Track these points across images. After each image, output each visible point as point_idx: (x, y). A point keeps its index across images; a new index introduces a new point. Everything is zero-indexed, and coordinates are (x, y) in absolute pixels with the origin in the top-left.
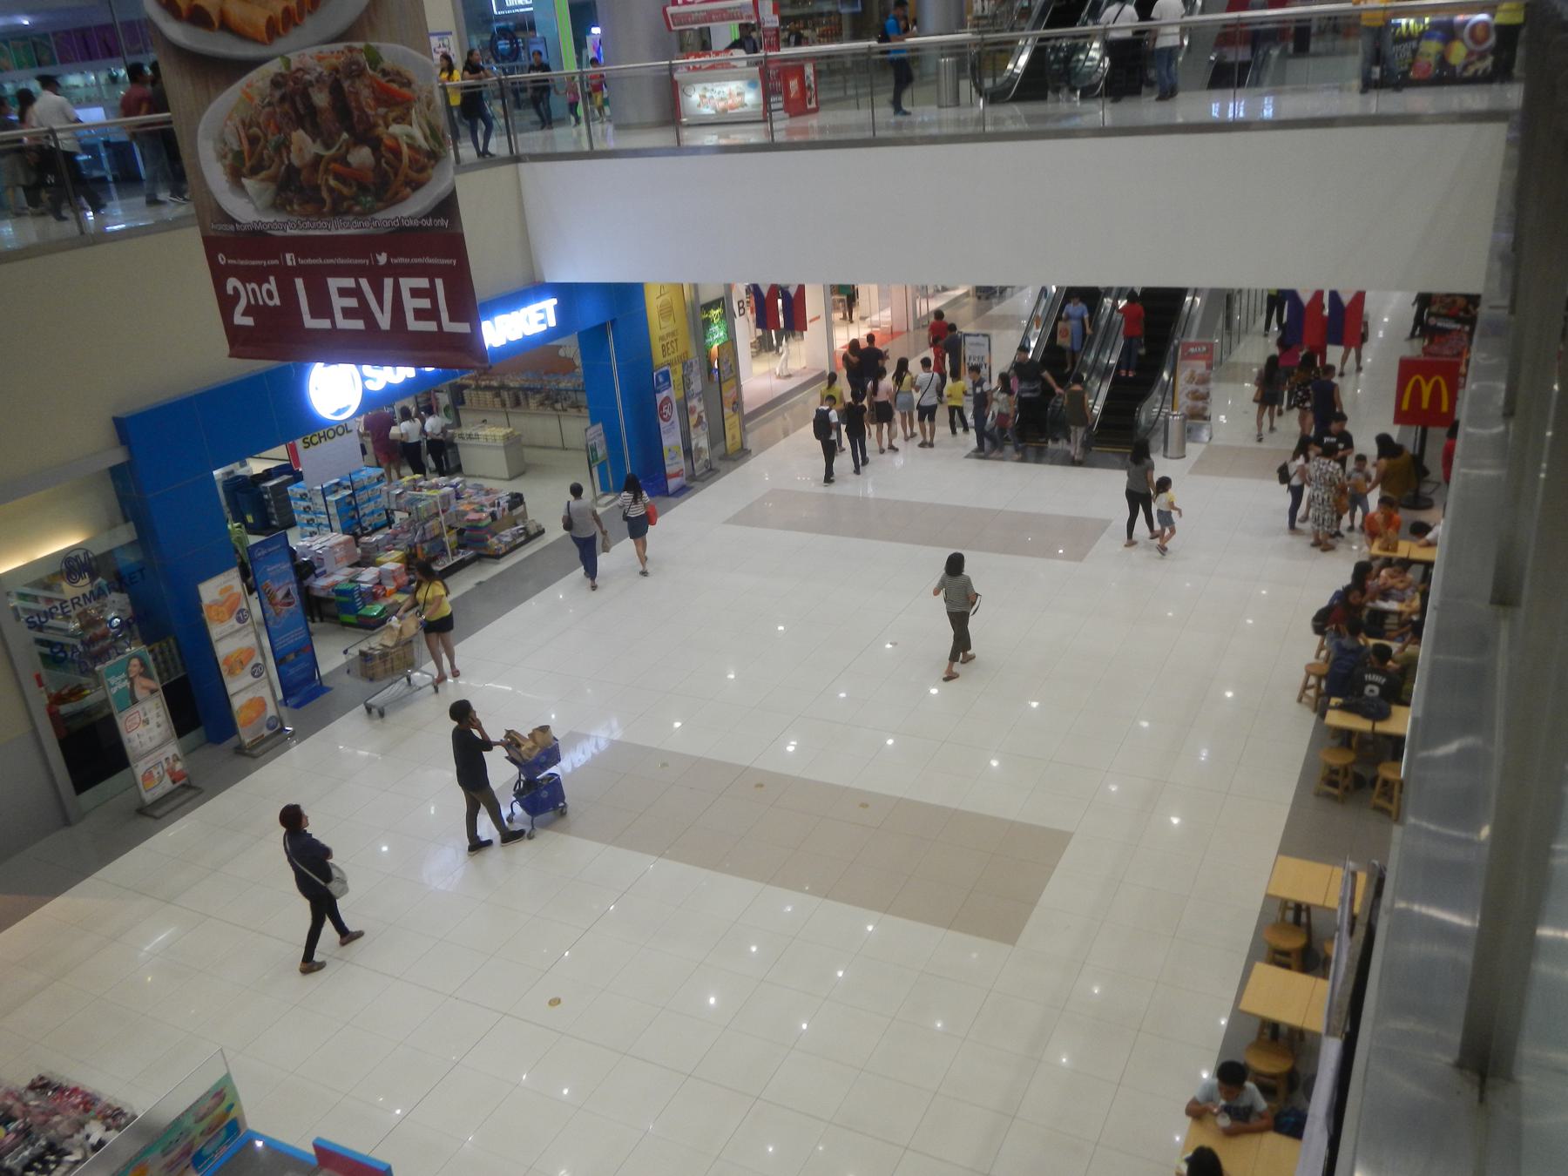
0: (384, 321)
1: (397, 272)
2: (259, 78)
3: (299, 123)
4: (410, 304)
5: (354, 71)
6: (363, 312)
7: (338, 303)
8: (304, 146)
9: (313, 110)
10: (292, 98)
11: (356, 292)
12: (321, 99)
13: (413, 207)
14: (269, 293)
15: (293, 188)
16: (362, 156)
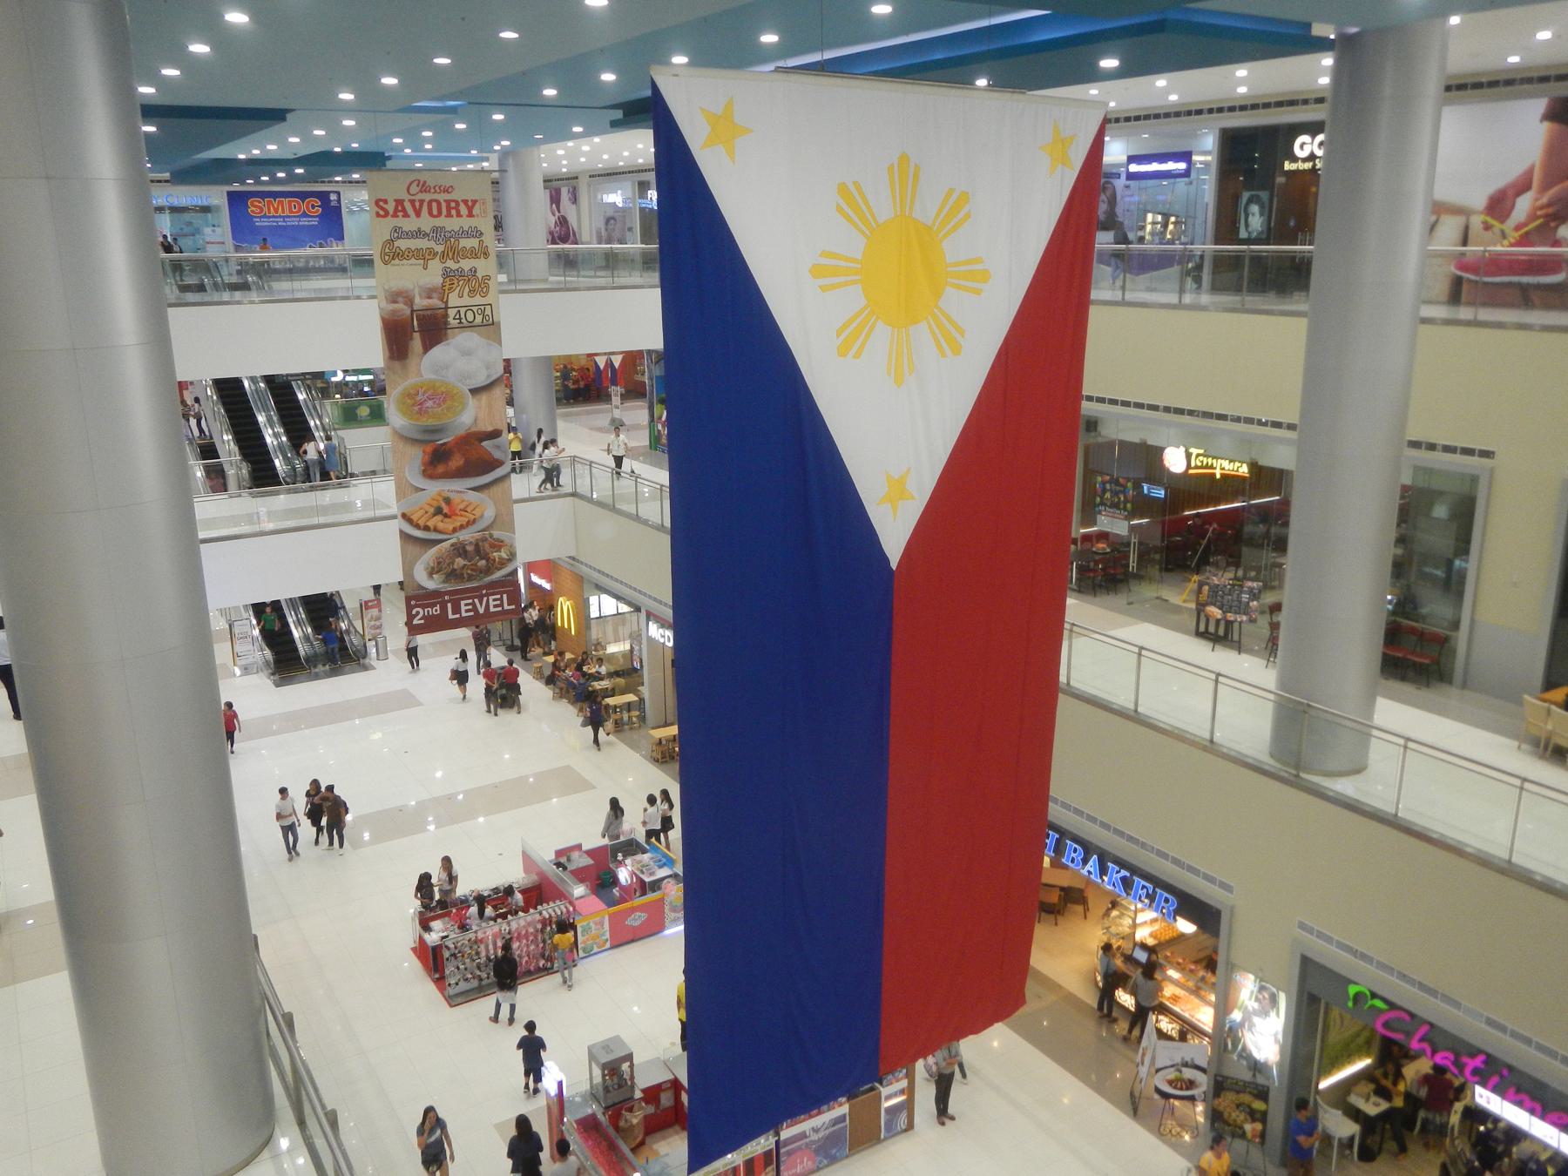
0: (481, 611)
1: (488, 595)
2: (446, 545)
3: (460, 555)
4: (492, 603)
5: (484, 540)
6: (475, 609)
7: (463, 608)
8: (460, 562)
9: (466, 552)
10: (460, 550)
11: (473, 604)
12: (470, 548)
13: (498, 575)
14: (436, 610)
15: (453, 575)
16: (483, 562)
